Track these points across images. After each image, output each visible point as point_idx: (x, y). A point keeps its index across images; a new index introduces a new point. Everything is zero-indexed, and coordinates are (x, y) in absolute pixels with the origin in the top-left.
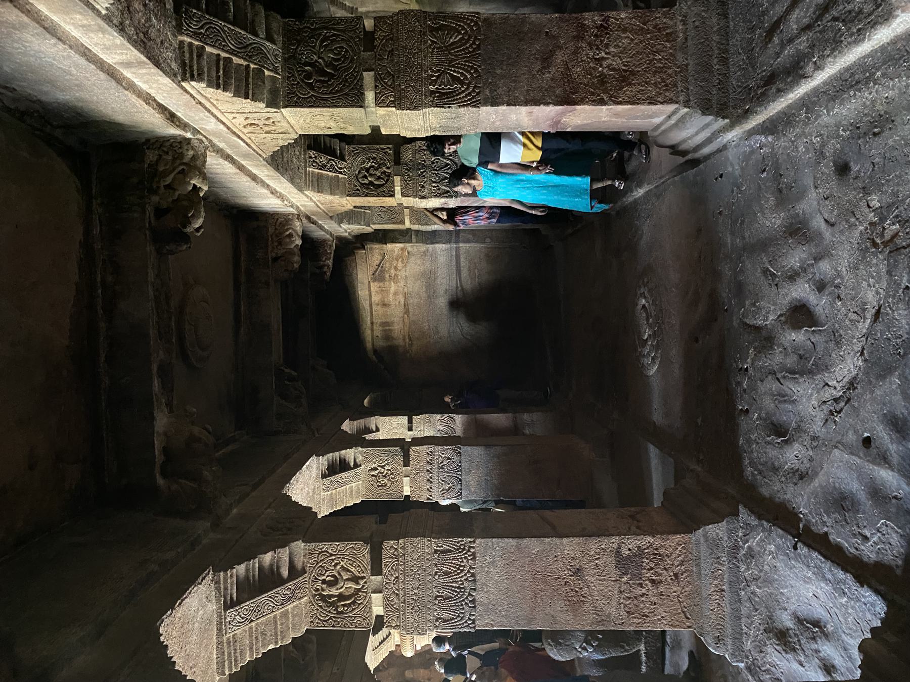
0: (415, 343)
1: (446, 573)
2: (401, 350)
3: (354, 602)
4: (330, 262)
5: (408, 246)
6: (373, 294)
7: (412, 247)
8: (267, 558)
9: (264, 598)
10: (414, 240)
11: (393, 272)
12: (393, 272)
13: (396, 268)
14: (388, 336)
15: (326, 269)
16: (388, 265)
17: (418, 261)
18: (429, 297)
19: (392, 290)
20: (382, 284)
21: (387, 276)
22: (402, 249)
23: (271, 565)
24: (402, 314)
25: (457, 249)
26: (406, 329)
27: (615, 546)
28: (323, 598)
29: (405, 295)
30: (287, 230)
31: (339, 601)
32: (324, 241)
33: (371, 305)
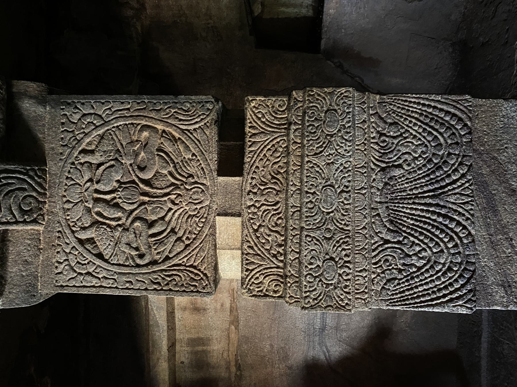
0: (246, 373)
14: (200, 361)
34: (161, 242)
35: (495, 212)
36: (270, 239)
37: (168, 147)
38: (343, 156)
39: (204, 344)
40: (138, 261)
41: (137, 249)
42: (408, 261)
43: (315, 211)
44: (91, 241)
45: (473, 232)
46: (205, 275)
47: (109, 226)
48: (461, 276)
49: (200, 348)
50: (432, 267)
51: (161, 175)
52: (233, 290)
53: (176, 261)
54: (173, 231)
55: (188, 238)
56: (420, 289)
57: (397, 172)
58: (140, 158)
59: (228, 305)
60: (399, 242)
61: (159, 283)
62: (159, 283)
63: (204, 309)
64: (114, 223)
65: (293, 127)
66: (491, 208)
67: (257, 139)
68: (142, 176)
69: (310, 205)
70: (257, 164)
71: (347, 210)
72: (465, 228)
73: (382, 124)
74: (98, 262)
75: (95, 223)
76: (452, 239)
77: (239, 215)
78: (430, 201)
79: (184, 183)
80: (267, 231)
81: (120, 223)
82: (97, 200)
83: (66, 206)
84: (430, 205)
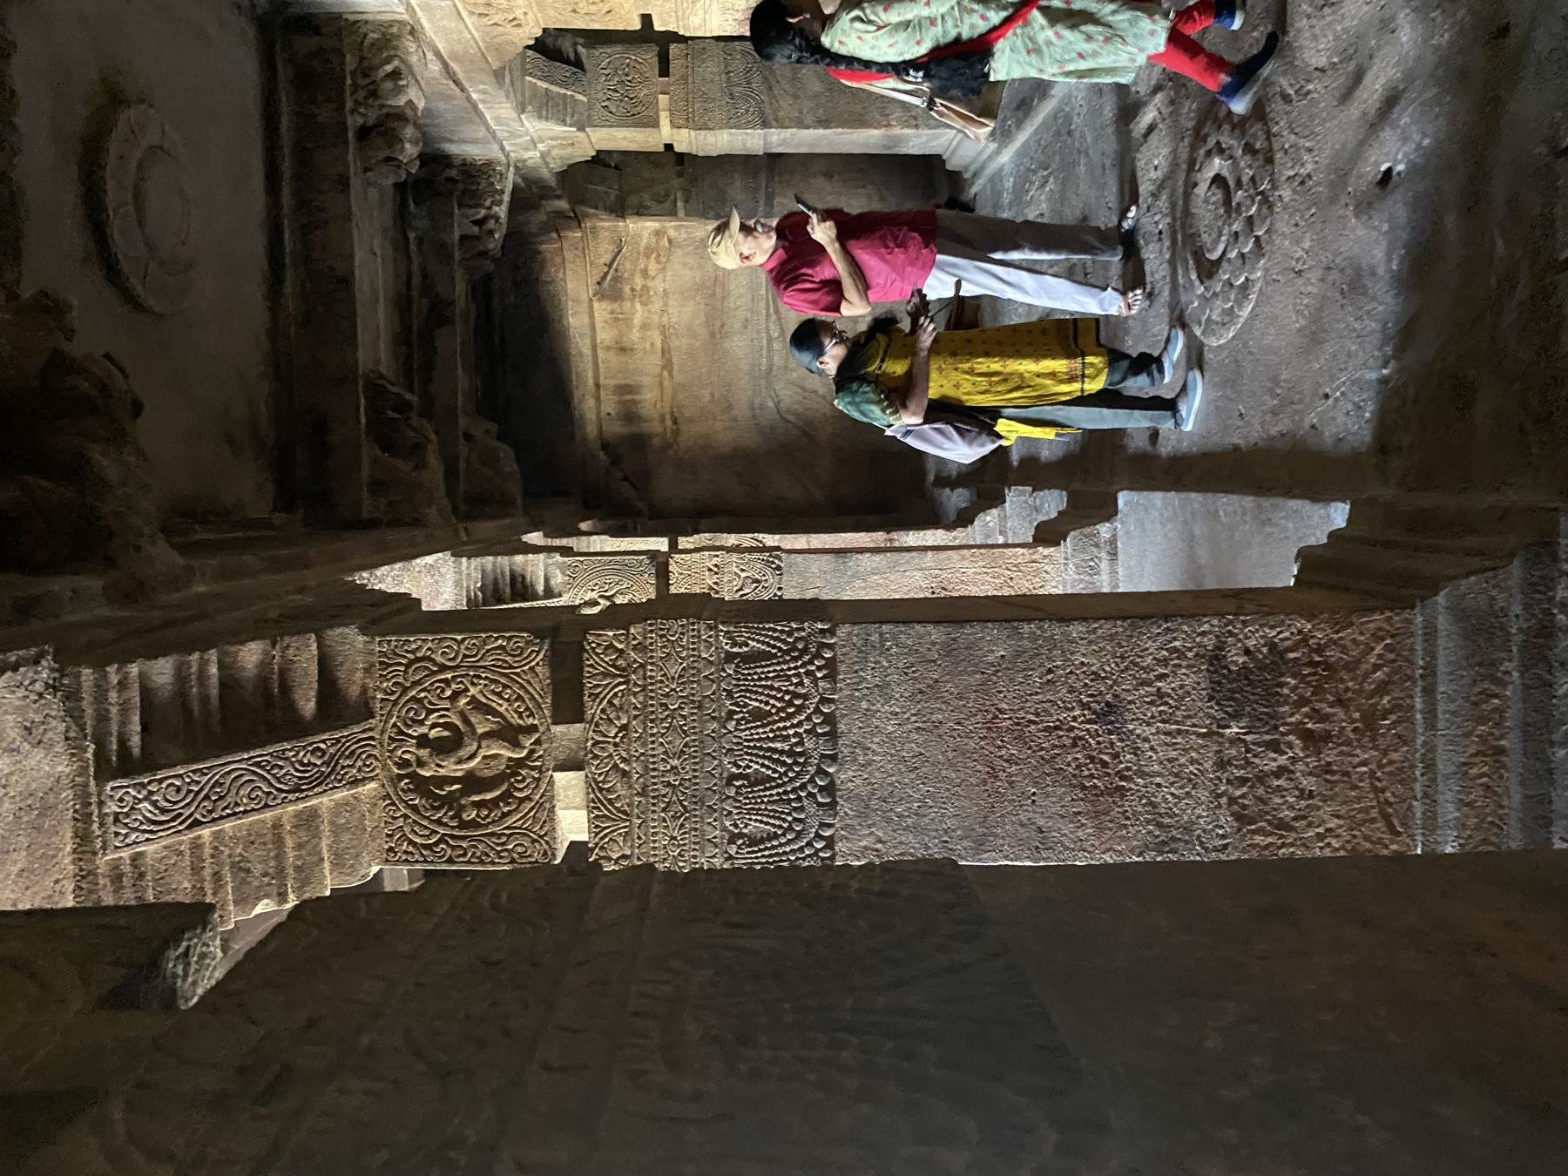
0: (683, 427)
1: (758, 715)
2: (656, 441)
3: (506, 796)
4: (502, 211)
5: (671, 227)
6: (599, 326)
7: (677, 228)
8: (251, 655)
9: (236, 763)
10: (681, 213)
11: (639, 281)
12: (639, 281)
13: (645, 273)
14: (630, 414)
15: (491, 224)
16: (628, 265)
17: (690, 260)
18: (712, 335)
20: (616, 305)
21: (627, 289)
22: (657, 233)
23: (263, 679)
24: (657, 370)
26: (667, 399)
27: (1209, 642)
28: (422, 786)
29: (663, 330)
30: (388, 61)
31: (465, 792)
32: (489, 164)
33: (594, 347)
39: (631, 393)
49: (629, 397)
66: (770, 88)
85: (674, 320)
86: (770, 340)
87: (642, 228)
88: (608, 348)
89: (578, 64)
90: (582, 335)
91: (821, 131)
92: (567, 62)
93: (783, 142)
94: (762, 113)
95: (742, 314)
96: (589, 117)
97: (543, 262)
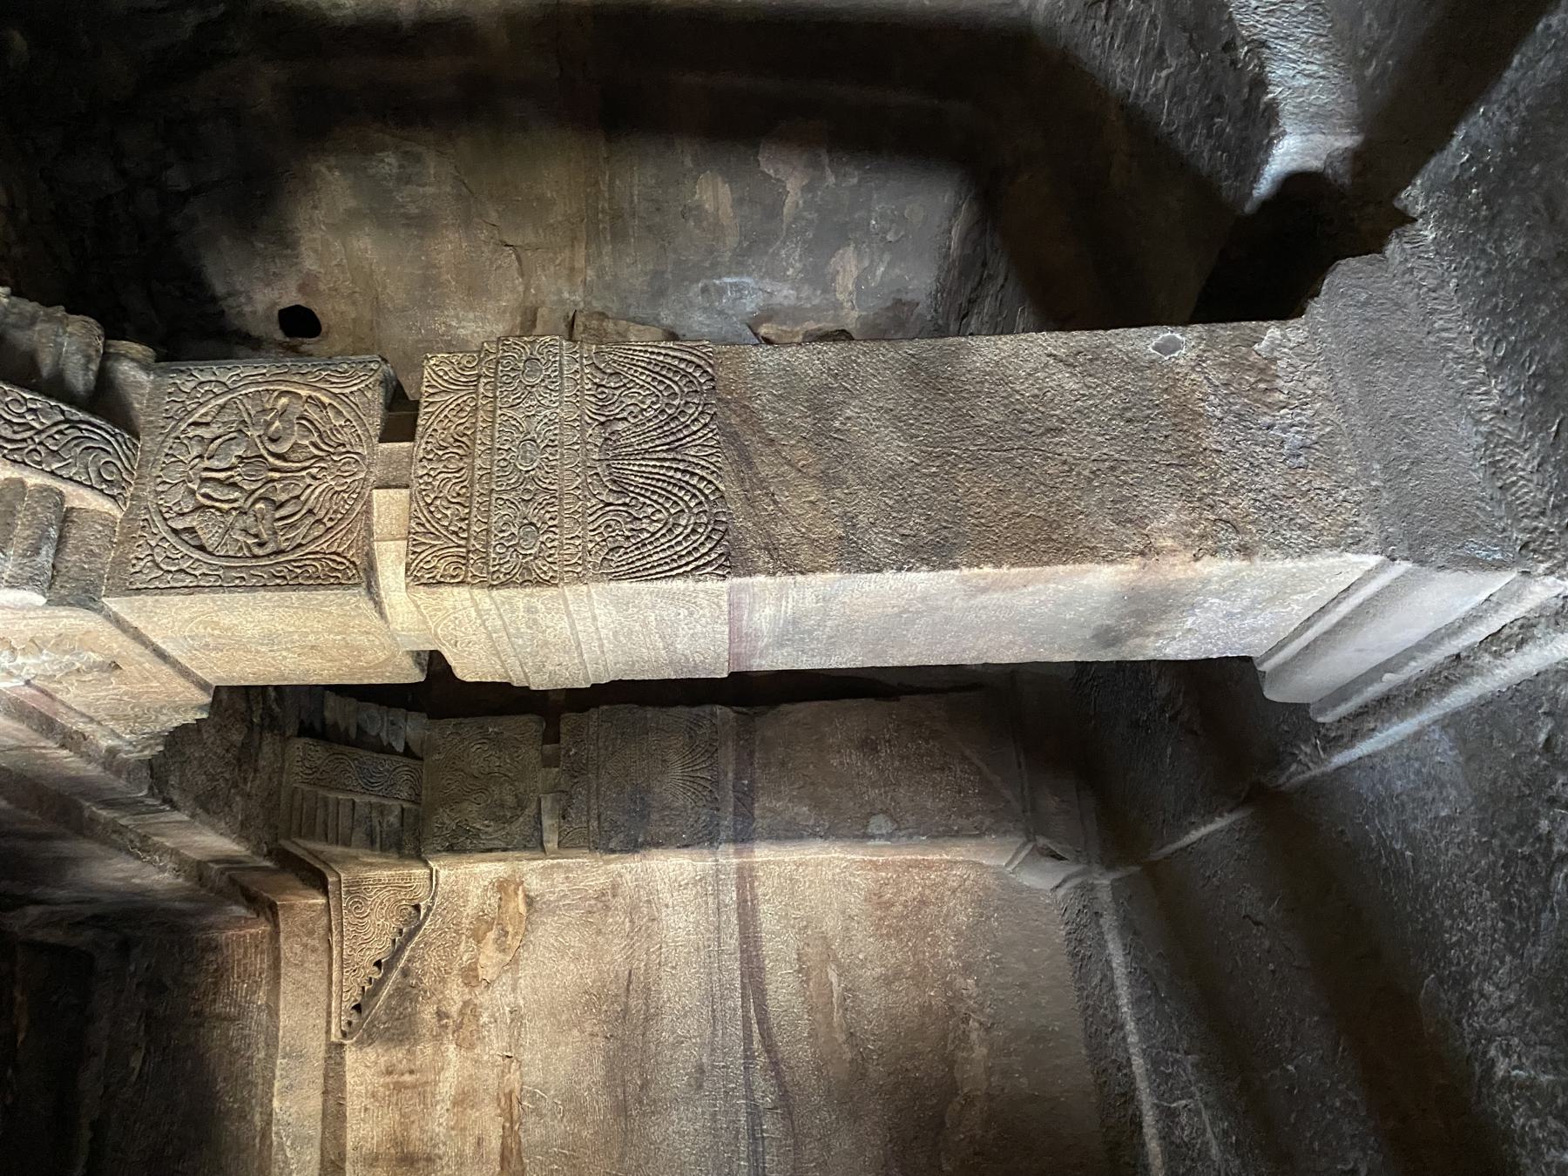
5: (533, 872)
6: (353, 1105)
7: (546, 873)
10: (551, 841)
12: (455, 994)
13: (470, 975)
16: (433, 959)
18: (621, 1109)
19: (447, 1086)
21: (427, 1013)
22: (502, 886)
25: (745, 877)
29: (509, 1104)
34: (292, 526)
35: (750, 465)
36: (448, 513)
37: (314, 414)
38: (548, 407)
40: (257, 551)
41: (256, 536)
42: (637, 525)
43: (510, 469)
44: (191, 530)
45: (722, 487)
46: (353, 563)
47: (218, 509)
48: (709, 537)
50: (670, 530)
51: (300, 446)
52: (509, 1095)
53: (312, 548)
54: (310, 511)
55: (331, 519)
56: (655, 557)
57: (621, 426)
58: (273, 428)
59: (495, 1143)
60: (624, 504)
61: (284, 578)
62: (284, 578)
63: (429, 1159)
64: (226, 506)
65: (483, 380)
67: (437, 398)
68: (272, 448)
69: (502, 464)
70: (435, 426)
71: (552, 467)
72: (710, 482)
73: (599, 375)
74: (196, 555)
75: (200, 508)
76: (694, 496)
77: (407, 487)
78: (665, 455)
79: (329, 454)
80: (445, 504)
81: (235, 505)
82: (205, 480)
83: (159, 489)
84: (665, 460)
85: (535, 1077)
86: (754, 1113)
87: (469, 879)
88: (372, 1160)
89: (105, 401)
90: (300, 1141)
91: (922, 580)
92: (56, 388)
93: (792, 630)
94: (719, 530)
95: (690, 1054)
96: (120, 563)
97: (221, 973)
